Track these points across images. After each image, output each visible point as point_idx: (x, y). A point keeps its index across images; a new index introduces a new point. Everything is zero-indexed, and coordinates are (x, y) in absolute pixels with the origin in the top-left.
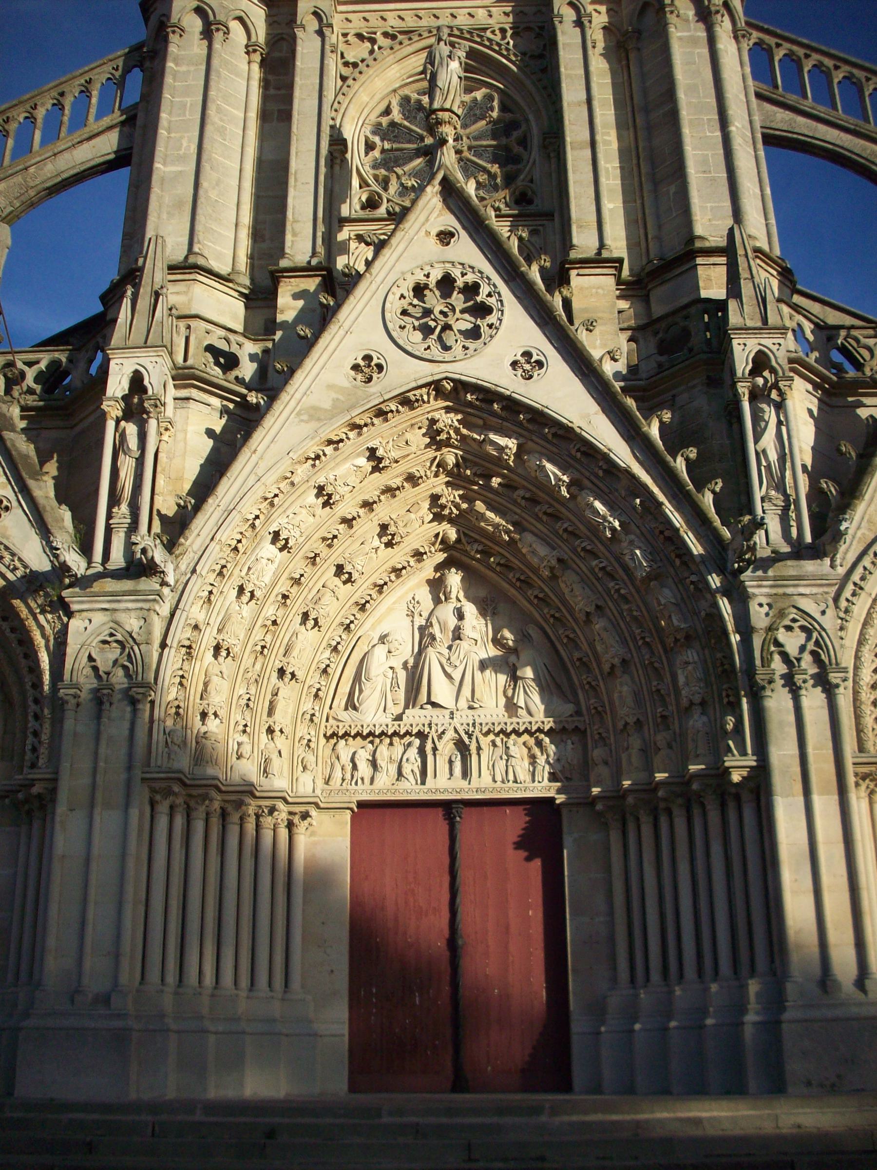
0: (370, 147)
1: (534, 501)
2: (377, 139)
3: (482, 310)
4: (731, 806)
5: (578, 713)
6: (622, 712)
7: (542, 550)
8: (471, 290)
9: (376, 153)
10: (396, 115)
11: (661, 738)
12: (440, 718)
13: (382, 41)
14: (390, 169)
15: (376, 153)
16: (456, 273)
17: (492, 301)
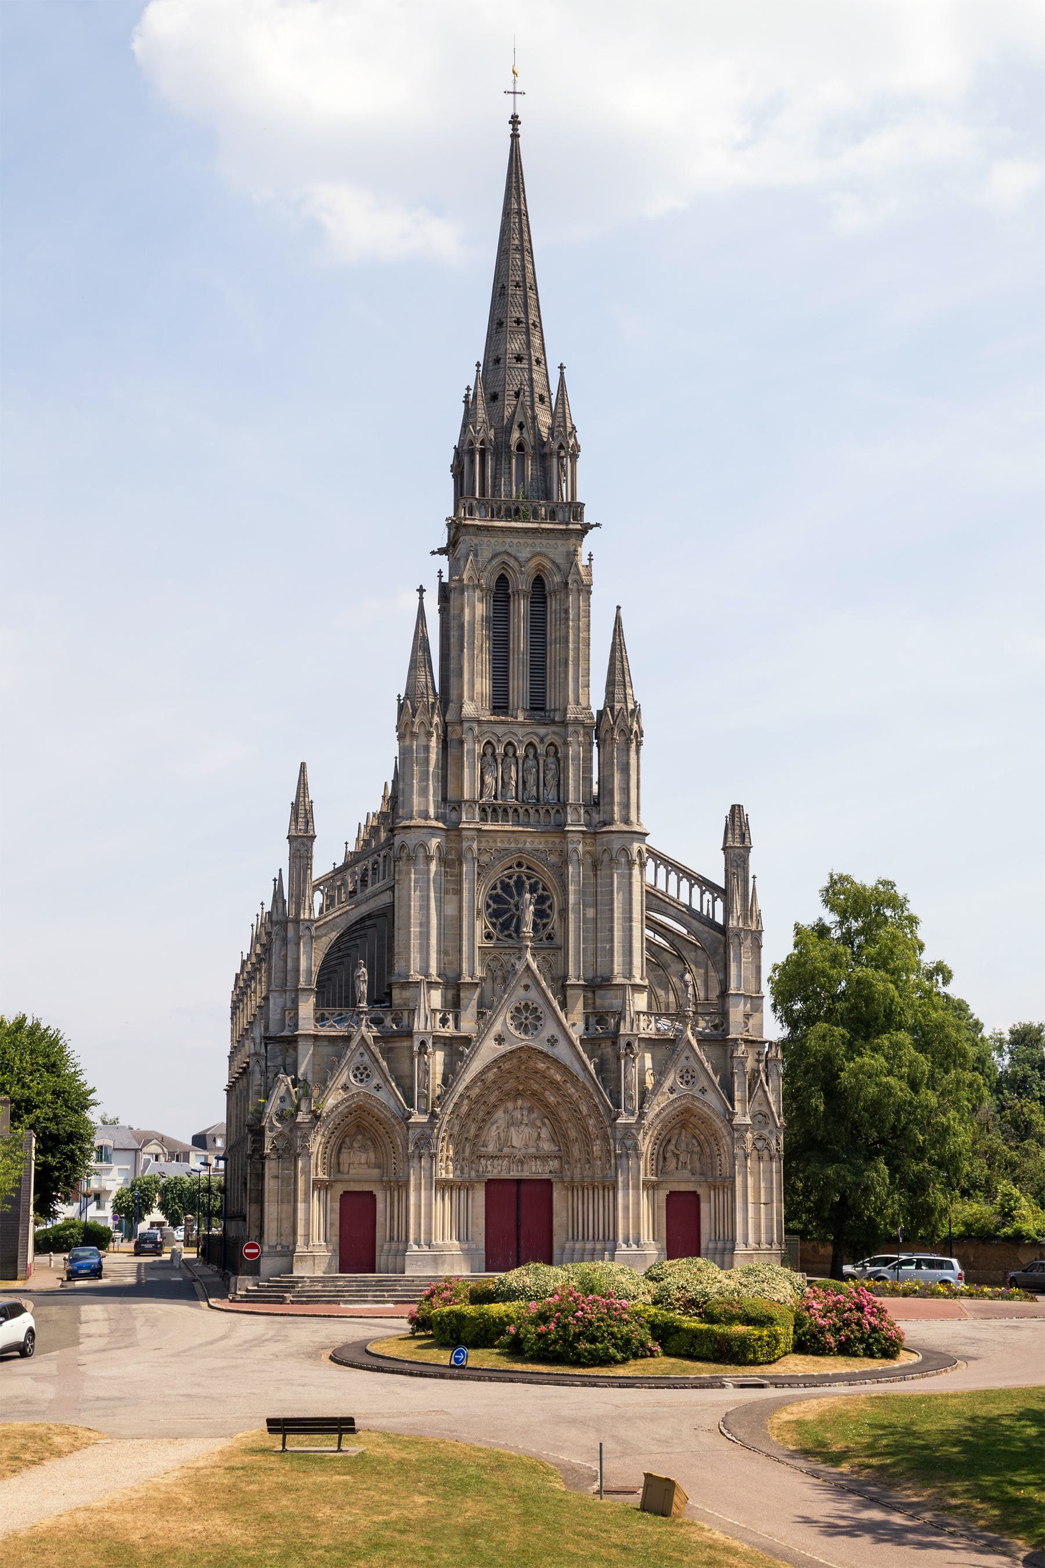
0: (488, 906)
1: (551, 1083)
2: (491, 902)
3: (539, 1018)
4: (606, 1190)
5: (560, 1150)
6: (575, 1154)
7: (552, 1098)
8: (537, 1008)
9: (490, 910)
10: (499, 891)
11: (587, 1166)
12: (515, 1151)
13: (495, 854)
14: (497, 918)
15: (490, 910)
16: (530, 1003)
17: (542, 1015)
